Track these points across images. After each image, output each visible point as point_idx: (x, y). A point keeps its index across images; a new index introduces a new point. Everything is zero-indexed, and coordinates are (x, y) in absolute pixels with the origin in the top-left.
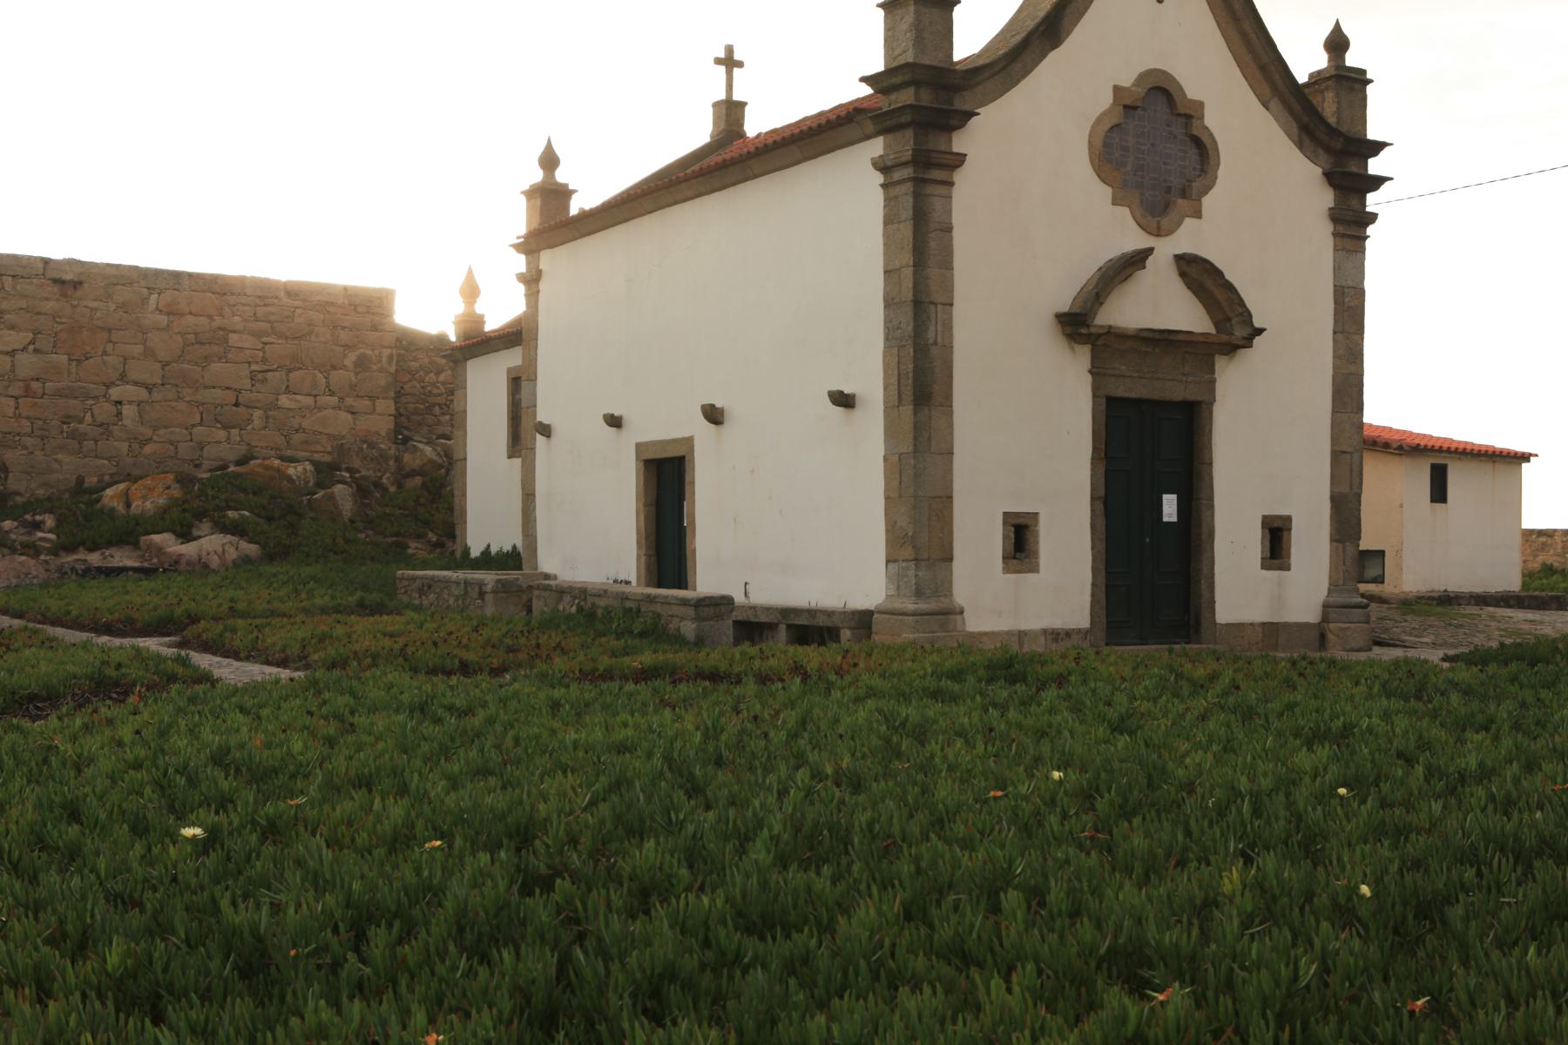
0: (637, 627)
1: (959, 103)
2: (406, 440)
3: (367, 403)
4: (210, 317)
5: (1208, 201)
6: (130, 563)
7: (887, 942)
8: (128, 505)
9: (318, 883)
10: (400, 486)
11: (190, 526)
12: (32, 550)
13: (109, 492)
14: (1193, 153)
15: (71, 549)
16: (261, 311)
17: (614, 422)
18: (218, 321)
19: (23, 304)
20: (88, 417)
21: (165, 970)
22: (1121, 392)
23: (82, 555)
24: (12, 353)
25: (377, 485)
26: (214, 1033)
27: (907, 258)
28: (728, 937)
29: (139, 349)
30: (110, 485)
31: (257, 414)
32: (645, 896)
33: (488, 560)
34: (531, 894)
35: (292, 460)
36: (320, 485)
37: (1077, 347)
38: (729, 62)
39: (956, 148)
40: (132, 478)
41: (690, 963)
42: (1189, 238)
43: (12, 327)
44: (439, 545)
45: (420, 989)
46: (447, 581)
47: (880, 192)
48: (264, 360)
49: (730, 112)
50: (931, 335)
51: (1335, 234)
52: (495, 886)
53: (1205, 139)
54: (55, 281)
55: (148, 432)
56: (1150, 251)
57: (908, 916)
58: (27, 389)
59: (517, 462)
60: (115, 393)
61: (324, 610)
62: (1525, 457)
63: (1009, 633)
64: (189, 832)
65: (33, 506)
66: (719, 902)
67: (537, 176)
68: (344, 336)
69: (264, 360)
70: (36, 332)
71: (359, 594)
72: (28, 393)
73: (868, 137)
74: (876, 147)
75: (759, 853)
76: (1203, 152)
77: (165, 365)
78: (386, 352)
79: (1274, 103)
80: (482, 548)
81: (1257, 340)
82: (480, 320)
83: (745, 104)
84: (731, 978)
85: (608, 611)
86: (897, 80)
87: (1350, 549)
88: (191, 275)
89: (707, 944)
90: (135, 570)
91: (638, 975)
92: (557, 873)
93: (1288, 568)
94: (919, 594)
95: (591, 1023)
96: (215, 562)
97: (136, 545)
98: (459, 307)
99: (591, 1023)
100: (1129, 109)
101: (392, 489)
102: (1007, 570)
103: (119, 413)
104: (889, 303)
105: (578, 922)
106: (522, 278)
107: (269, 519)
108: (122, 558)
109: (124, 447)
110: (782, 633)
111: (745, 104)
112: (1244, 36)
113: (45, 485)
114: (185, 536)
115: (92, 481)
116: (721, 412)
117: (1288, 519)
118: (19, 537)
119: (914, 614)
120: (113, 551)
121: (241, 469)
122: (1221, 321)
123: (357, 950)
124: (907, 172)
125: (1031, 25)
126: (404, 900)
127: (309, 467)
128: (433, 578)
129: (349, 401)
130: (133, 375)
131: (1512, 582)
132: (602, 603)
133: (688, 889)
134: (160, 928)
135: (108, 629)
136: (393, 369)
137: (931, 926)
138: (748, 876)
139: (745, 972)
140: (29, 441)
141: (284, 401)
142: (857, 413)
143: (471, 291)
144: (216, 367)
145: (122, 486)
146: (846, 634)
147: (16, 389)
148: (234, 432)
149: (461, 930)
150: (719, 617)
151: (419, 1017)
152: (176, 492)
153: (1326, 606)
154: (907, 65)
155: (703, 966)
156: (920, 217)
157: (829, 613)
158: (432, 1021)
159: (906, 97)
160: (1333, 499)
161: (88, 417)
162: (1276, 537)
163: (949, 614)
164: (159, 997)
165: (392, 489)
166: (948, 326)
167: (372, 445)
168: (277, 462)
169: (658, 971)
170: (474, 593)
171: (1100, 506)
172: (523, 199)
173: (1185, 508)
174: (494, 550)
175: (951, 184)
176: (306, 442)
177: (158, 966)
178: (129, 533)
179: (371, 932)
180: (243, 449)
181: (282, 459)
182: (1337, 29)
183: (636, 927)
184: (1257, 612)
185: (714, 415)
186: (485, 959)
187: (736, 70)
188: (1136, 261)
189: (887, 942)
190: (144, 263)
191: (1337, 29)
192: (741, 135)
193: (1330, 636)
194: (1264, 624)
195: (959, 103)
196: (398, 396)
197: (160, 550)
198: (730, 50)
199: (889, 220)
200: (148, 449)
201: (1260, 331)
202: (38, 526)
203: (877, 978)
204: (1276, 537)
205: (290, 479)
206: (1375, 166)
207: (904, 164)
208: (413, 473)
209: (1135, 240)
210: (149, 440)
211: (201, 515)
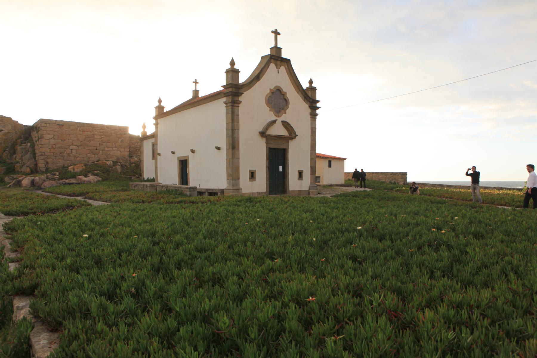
0: (178, 193)
1: (240, 91)
2: (131, 157)
3: (123, 149)
4: (91, 132)
5: (287, 111)
6: (74, 182)
7: (225, 253)
8: (74, 170)
9: (112, 245)
10: (130, 166)
11: (87, 174)
12: (54, 179)
13: (70, 167)
14: (285, 101)
15: (62, 179)
16: (101, 131)
18: (92, 133)
19: (51, 129)
20: (65, 152)
21: (80, 263)
22: (271, 147)
23: (64, 180)
24: (49, 139)
25: (126, 166)
26: (90, 276)
27: (230, 121)
28: (194, 253)
29: (76, 138)
30: (70, 166)
31: (101, 151)
32: (178, 245)
33: (148, 180)
34: (155, 246)
35: (108, 161)
36: (114, 166)
37: (263, 138)
38: (196, 82)
39: (240, 100)
40: (75, 165)
41: (186, 258)
42: (284, 117)
43: (49, 134)
44: (138, 177)
45: (132, 265)
46: (140, 185)
47: (225, 108)
48: (102, 141)
49: (196, 92)
50: (235, 136)
51: (311, 117)
52: (147, 244)
53: (287, 99)
54: (58, 125)
55: (78, 155)
56: (276, 120)
57: (229, 247)
58: (52, 147)
59: (154, 161)
60: (71, 147)
61: (115, 191)
62: (345, 159)
63: (251, 193)
64: (85, 235)
65: (54, 170)
66: (192, 246)
69: (102, 141)
70: (54, 135)
71: (122, 187)
72: (52, 147)
73: (223, 97)
74: (224, 99)
75: (200, 236)
76: (286, 101)
77: (81, 142)
78: (127, 139)
79: (300, 93)
80: (147, 178)
81: (297, 137)
82: (146, 133)
84: (194, 260)
85: (172, 190)
86: (228, 86)
87: (314, 176)
88: (87, 124)
89: (190, 254)
90: (76, 183)
91: (176, 261)
92: (160, 242)
93: (302, 180)
94: (233, 186)
95: (166, 270)
96: (92, 181)
97: (76, 178)
98: (142, 130)
99: (166, 270)
100: (273, 93)
101: (129, 166)
102: (250, 181)
103: (72, 152)
104: (227, 129)
105: (164, 251)
106: (154, 124)
107: (103, 173)
108: (73, 181)
109: (73, 158)
110: (207, 194)
112: (294, 80)
113: (56, 166)
114: (86, 176)
115: (66, 165)
116: (194, 151)
117: (303, 171)
118: (51, 177)
119: (232, 190)
120: (71, 179)
121: (97, 163)
122: (290, 133)
123: (119, 258)
124: (230, 104)
125: (254, 77)
126: (129, 248)
127: (112, 162)
128: (137, 184)
129: (120, 149)
131: (343, 182)
132: (171, 188)
133: (186, 244)
134: (78, 255)
135: (70, 195)
136: (128, 142)
137: (233, 249)
138: (198, 241)
139: (197, 259)
140: (53, 157)
141: (106, 149)
142: (221, 151)
143: (144, 127)
144: (92, 142)
145: (73, 166)
146: (219, 194)
147: (50, 147)
148: (96, 155)
149: (140, 253)
150: (194, 191)
151: (132, 271)
152: (84, 167)
153: (310, 187)
154: (230, 84)
155: (189, 259)
156: (233, 113)
157: (216, 190)
158: (134, 271)
159: (230, 90)
160: (311, 167)
161: (65, 152)
162: (300, 174)
163: (239, 189)
164: (78, 269)
165: (129, 166)
166: (238, 134)
167: (124, 158)
168: (105, 161)
169: (180, 260)
170: (145, 187)
171: (268, 169)
173: (284, 169)
174: (149, 178)
175: (239, 107)
176: (111, 157)
177: (78, 263)
178: (74, 176)
179: (122, 254)
180: (98, 159)
181: (106, 160)
182: (233, 60)
183: (176, 252)
184: (297, 189)
185: (193, 151)
186: (145, 259)
187: (197, 84)
188: (274, 122)
189: (225, 253)
190: (77, 121)
191: (233, 60)
192: (198, 97)
193: (310, 193)
194: (298, 191)
195: (240, 91)
196: (130, 148)
197: (81, 179)
198: (196, 80)
199: (227, 113)
200: (78, 159)
201: (297, 135)
202: (55, 175)
203: (223, 259)
204: (300, 174)
205: (108, 165)
207: (230, 103)
208: (133, 163)
209: (274, 118)
210: (78, 157)
211: (89, 172)
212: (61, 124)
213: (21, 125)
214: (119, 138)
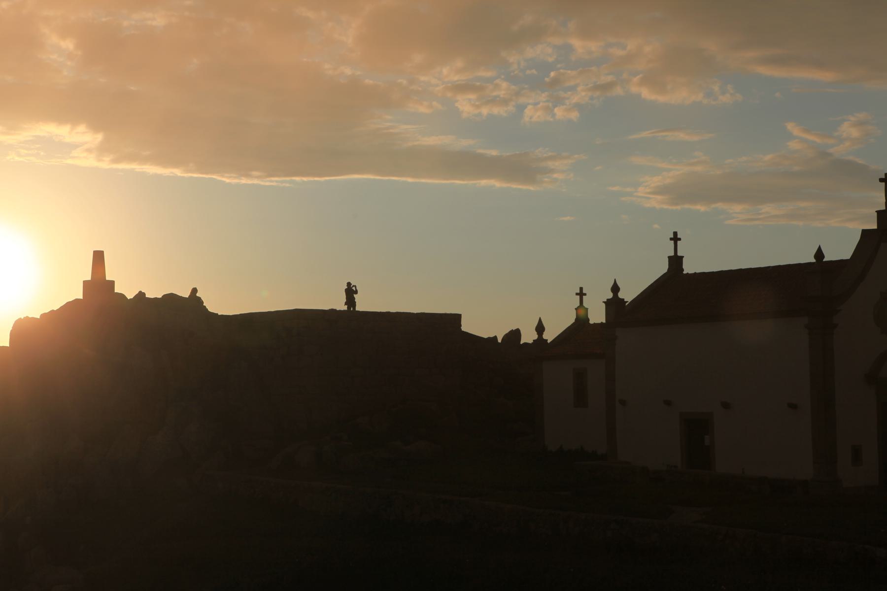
17: (668, 403)
49: (676, 261)
67: (610, 295)
83: (683, 257)
111: (683, 257)
172: (604, 305)
185: (726, 406)
187: (679, 242)
198: (675, 234)
213: (215, 315)
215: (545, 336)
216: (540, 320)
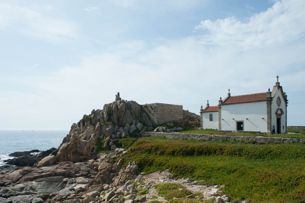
8: (170, 125)
17: (233, 119)
49: (229, 94)
68: (180, 110)
70: (160, 110)
74: (266, 102)
130: (167, 113)
141: (176, 116)
190: (167, 104)
198: (229, 89)
206: (288, 102)
212: (162, 105)
214: (180, 111)
215: (203, 108)
216: (269, 88)
